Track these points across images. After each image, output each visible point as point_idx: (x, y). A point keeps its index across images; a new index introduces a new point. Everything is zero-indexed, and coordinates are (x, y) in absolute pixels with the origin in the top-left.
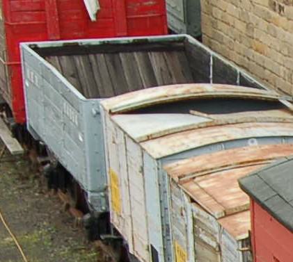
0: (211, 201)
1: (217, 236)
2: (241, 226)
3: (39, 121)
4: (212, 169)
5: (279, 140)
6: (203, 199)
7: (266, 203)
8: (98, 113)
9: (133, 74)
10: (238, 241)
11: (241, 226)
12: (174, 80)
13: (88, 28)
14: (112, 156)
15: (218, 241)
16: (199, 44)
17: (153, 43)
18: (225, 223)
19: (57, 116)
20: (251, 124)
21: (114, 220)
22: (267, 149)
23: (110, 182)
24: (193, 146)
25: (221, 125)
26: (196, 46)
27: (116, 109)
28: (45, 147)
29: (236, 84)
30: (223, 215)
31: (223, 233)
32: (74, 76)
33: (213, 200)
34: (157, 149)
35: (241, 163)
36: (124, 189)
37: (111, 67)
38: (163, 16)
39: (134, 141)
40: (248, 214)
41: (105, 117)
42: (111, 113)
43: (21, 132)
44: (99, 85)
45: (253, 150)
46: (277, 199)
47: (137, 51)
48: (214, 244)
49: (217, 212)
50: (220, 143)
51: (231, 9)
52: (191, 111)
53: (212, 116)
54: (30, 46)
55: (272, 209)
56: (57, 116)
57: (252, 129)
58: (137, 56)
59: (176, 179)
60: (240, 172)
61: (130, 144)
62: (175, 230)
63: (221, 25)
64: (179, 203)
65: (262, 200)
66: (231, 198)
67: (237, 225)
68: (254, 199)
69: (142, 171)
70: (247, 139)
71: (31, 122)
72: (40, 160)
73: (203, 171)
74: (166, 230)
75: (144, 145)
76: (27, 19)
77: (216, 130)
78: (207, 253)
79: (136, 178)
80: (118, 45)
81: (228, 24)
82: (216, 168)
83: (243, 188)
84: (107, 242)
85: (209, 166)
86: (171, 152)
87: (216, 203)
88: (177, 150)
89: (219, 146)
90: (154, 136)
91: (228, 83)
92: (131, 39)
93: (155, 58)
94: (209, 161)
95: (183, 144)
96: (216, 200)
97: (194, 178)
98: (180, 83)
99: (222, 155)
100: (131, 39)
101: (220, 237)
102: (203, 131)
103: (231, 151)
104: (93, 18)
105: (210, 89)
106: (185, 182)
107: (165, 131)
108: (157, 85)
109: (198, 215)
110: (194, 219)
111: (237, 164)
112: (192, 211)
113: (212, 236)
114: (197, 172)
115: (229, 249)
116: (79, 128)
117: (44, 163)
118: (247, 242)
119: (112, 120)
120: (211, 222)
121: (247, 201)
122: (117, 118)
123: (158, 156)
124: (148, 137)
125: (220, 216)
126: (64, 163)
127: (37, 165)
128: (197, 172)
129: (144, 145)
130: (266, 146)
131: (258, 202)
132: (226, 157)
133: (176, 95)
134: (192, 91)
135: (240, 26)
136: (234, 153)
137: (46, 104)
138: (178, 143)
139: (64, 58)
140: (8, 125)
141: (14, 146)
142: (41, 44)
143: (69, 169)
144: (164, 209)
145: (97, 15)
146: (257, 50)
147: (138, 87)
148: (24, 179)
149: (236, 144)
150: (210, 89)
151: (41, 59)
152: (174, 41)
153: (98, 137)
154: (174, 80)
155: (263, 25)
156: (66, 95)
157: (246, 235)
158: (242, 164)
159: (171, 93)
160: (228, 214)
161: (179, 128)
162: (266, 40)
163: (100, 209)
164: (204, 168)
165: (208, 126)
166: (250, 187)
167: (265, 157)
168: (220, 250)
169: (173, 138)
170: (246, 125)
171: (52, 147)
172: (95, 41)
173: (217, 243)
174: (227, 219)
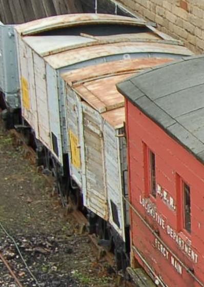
0: (96, 101)
1: (101, 126)
2: (118, 119)
4: (96, 76)
5: (146, 55)
6: (90, 98)
7: (136, 102)
8: (13, 35)
9: (39, 7)
10: (116, 130)
11: (118, 119)
12: (69, 11)
14: (23, 67)
15: (101, 129)
18: (106, 116)
20: (125, 43)
21: (25, 114)
22: (137, 62)
23: (21, 86)
25: (104, 44)
27: (26, 32)
29: (114, 14)
30: (105, 110)
31: (105, 123)
33: (97, 100)
34: (57, 62)
35: (118, 72)
36: (32, 91)
39: (39, 56)
40: (123, 109)
41: (18, 38)
42: (22, 35)
44: (14, 15)
45: (126, 62)
46: (145, 98)
48: (98, 132)
49: (101, 108)
50: (102, 57)
52: (82, 34)
53: (96, 37)
55: (141, 106)
57: (127, 47)
59: (70, 84)
60: (117, 79)
61: (36, 58)
62: (70, 121)
64: (72, 102)
65: (134, 99)
66: (111, 98)
67: (114, 117)
68: (127, 99)
69: (45, 78)
70: (123, 54)
73: (90, 78)
74: (63, 121)
75: (47, 59)
77: (99, 47)
78: (93, 138)
79: (41, 83)
82: (99, 76)
83: (120, 90)
84: (19, 130)
85: (95, 74)
86: (66, 64)
87: (99, 101)
88: (71, 63)
89: (102, 60)
90: (54, 52)
91: (109, 13)
94: (95, 70)
95: (75, 58)
96: (100, 100)
97: (83, 83)
98: (73, 13)
99: (104, 66)
101: (103, 127)
103: (110, 63)
105: (95, 17)
106: (77, 86)
107: (62, 48)
108: (56, 15)
109: (86, 110)
110: (83, 113)
111: (115, 73)
112: (82, 107)
113: (97, 126)
114: (86, 79)
115: (109, 135)
118: (123, 130)
119: (22, 40)
120: (96, 116)
121: (123, 100)
122: (26, 39)
123: (57, 67)
124: (50, 53)
125: (103, 111)
128: (86, 79)
129: (47, 59)
131: (131, 101)
132: (108, 68)
133: (70, 22)
134: (82, 19)
136: (113, 64)
138: (72, 57)
144: (61, 106)
147: (42, 16)
149: (114, 58)
150: (95, 17)
153: (12, 53)
154: (69, 11)
157: (122, 125)
158: (119, 73)
159: (66, 21)
160: (108, 110)
161: (72, 46)
163: (14, 106)
164: (91, 76)
165: (94, 45)
166: (124, 90)
167: (136, 68)
168: (103, 136)
169: (68, 54)
170: (122, 44)
173: (101, 131)
174: (108, 113)
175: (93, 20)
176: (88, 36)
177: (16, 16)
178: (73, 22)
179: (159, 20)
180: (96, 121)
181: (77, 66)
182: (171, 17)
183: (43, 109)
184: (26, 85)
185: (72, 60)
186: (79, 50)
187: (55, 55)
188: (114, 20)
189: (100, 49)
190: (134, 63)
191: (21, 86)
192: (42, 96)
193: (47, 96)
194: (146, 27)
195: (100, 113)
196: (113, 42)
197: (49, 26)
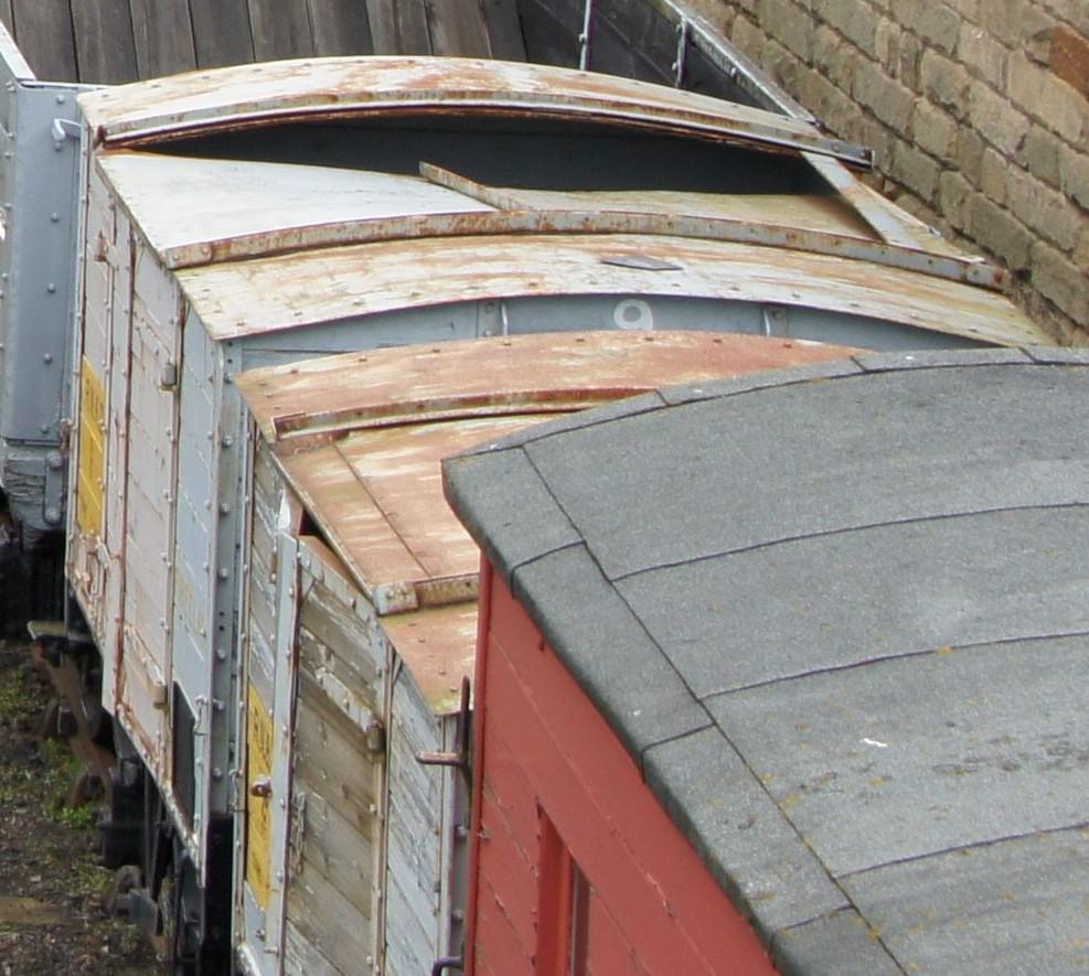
0: (383, 541)
1: (380, 687)
4: (421, 407)
6: (353, 526)
15: (381, 708)
22: (676, 350)
27: (127, 127)
30: (411, 599)
33: (390, 535)
34: (233, 302)
39: (161, 264)
48: (362, 718)
52: (425, 166)
53: (495, 193)
59: (269, 430)
69: (174, 381)
73: (382, 411)
75: (193, 283)
79: (153, 407)
82: (435, 405)
85: (417, 395)
87: (399, 546)
88: (310, 317)
89: (486, 319)
90: (234, 251)
95: (343, 294)
96: (401, 539)
97: (343, 435)
99: (479, 356)
102: (440, 250)
105: (520, 82)
106: (307, 447)
107: (285, 233)
109: (318, 585)
110: (301, 601)
111: (528, 397)
112: (300, 568)
113: (361, 684)
114: (359, 413)
120: (363, 625)
123: (235, 332)
124: (213, 247)
125: (399, 602)
128: (359, 413)
129: (193, 283)
130: (676, 339)
132: (500, 365)
133: (370, 96)
136: (534, 351)
138: (325, 286)
159: (358, 86)
161: (342, 226)
164: (395, 398)
165: (464, 230)
169: (313, 264)
173: (375, 716)
175: (508, 96)
176: (454, 179)
178: (388, 95)
180: (360, 658)
181: (342, 338)
183: (148, 554)
184: (96, 409)
185: (324, 299)
186: (375, 252)
187: (244, 267)
188: (618, 105)
189: (487, 260)
190: (659, 355)
191: (74, 413)
192: (152, 480)
193: (176, 482)
194: (805, 162)
195: (379, 615)
196: (575, 226)
197: (256, 105)
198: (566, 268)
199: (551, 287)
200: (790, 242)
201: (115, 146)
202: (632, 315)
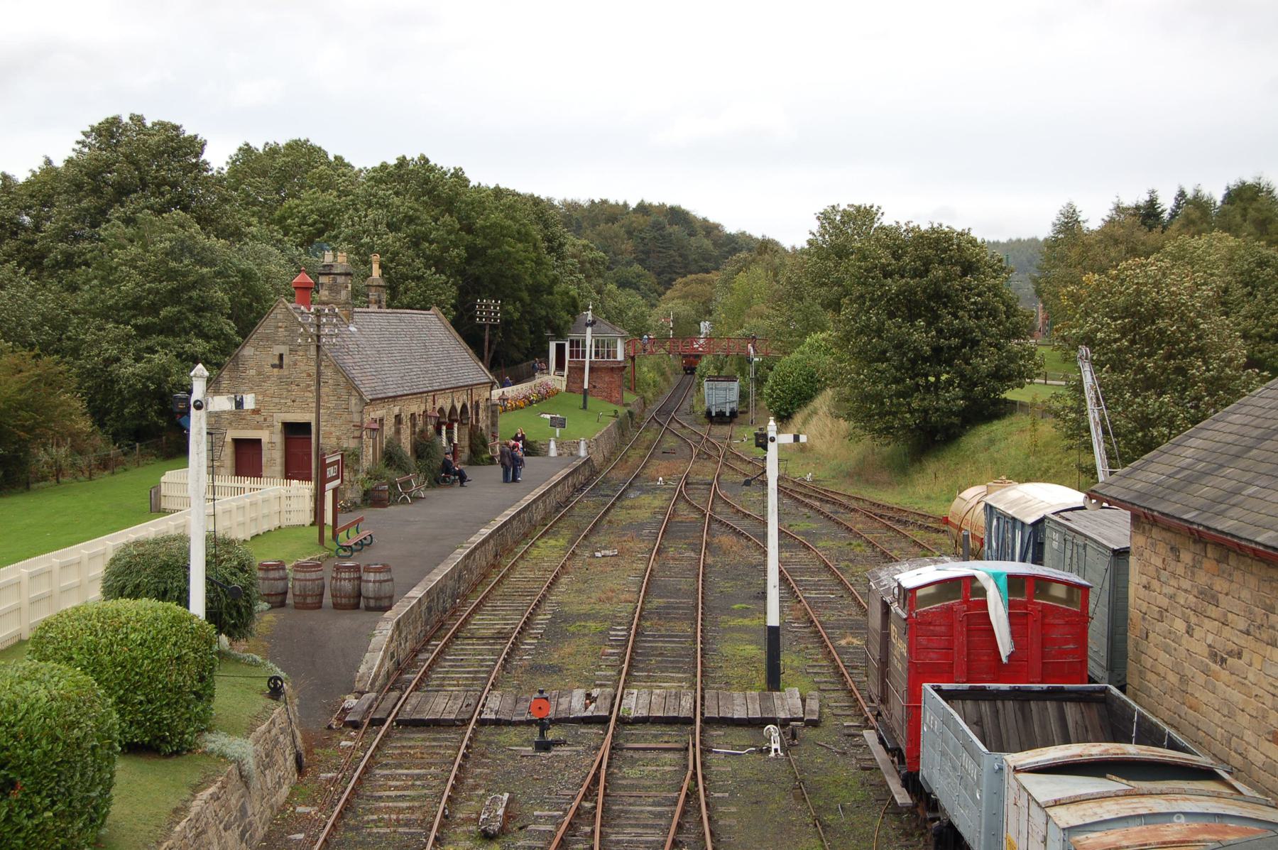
3: (933, 771)
8: (1001, 769)
9: (1044, 727)
12: (1090, 737)
13: (998, 670)
16: (1123, 696)
17: (1070, 691)
19: (954, 768)
24: (1107, 817)
25: (1143, 795)
26: (1119, 698)
28: (936, 802)
29: (1163, 747)
32: (977, 724)
37: (1019, 714)
38: (1084, 663)
42: (1016, 770)
43: (912, 782)
44: (1004, 736)
47: (1051, 700)
51: (1163, 657)
53: (1132, 783)
54: (933, 687)
56: (954, 768)
58: (1051, 706)
63: (1150, 676)
69: (1045, 841)
70: (1173, 814)
71: (924, 772)
72: (929, 815)
75: (1051, 812)
76: (933, 657)
77: (1135, 800)
80: (1030, 692)
81: (1158, 674)
86: (1081, 823)
88: (1088, 821)
89: (1138, 821)
92: (1045, 686)
93: (1071, 710)
94: (1125, 837)
98: (1097, 740)
99: (1141, 831)
100: (1045, 686)
102: (1121, 800)
103: (1151, 827)
104: (1004, 660)
105: (1132, 750)
108: (1069, 742)
116: (978, 784)
117: (933, 820)
119: (1017, 780)
126: (956, 822)
127: (925, 820)
129: (1051, 812)
135: (1173, 678)
136: (1156, 830)
137: (943, 754)
138: (1089, 812)
139: (969, 703)
140: (899, 772)
141: (902, 797)
142: (945, 686)
143: (961, 829)
145: (1009, 657)
146: (1191, 708)
147: (1048, 743)
148: (908, 835)
150: (1132, 750)
151: (944, 703)
152: (1094, 691)
153: (997, 795)
154: (1090, 737)
155: (1200, 678)
156: (968, 746)
159: (1087, 752)
162: (1204, 696)
165: (1127, 794)
169: (1085, 806)
171: (944, 802)
172: (1004, 686)
177: (1008, 738)
179: (1236, 760)
182: (1257, 757)
198: (1158, 805)
199: (1156, 810)
200: (1218, 796)
201: (1019, 771)
202: (1179, 818)
